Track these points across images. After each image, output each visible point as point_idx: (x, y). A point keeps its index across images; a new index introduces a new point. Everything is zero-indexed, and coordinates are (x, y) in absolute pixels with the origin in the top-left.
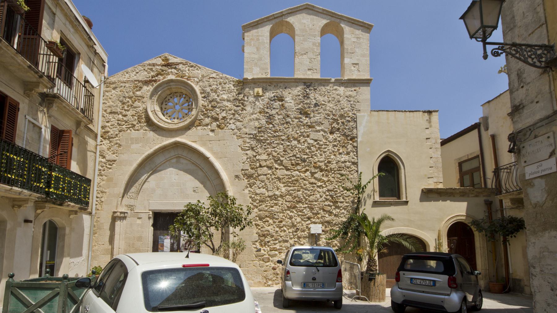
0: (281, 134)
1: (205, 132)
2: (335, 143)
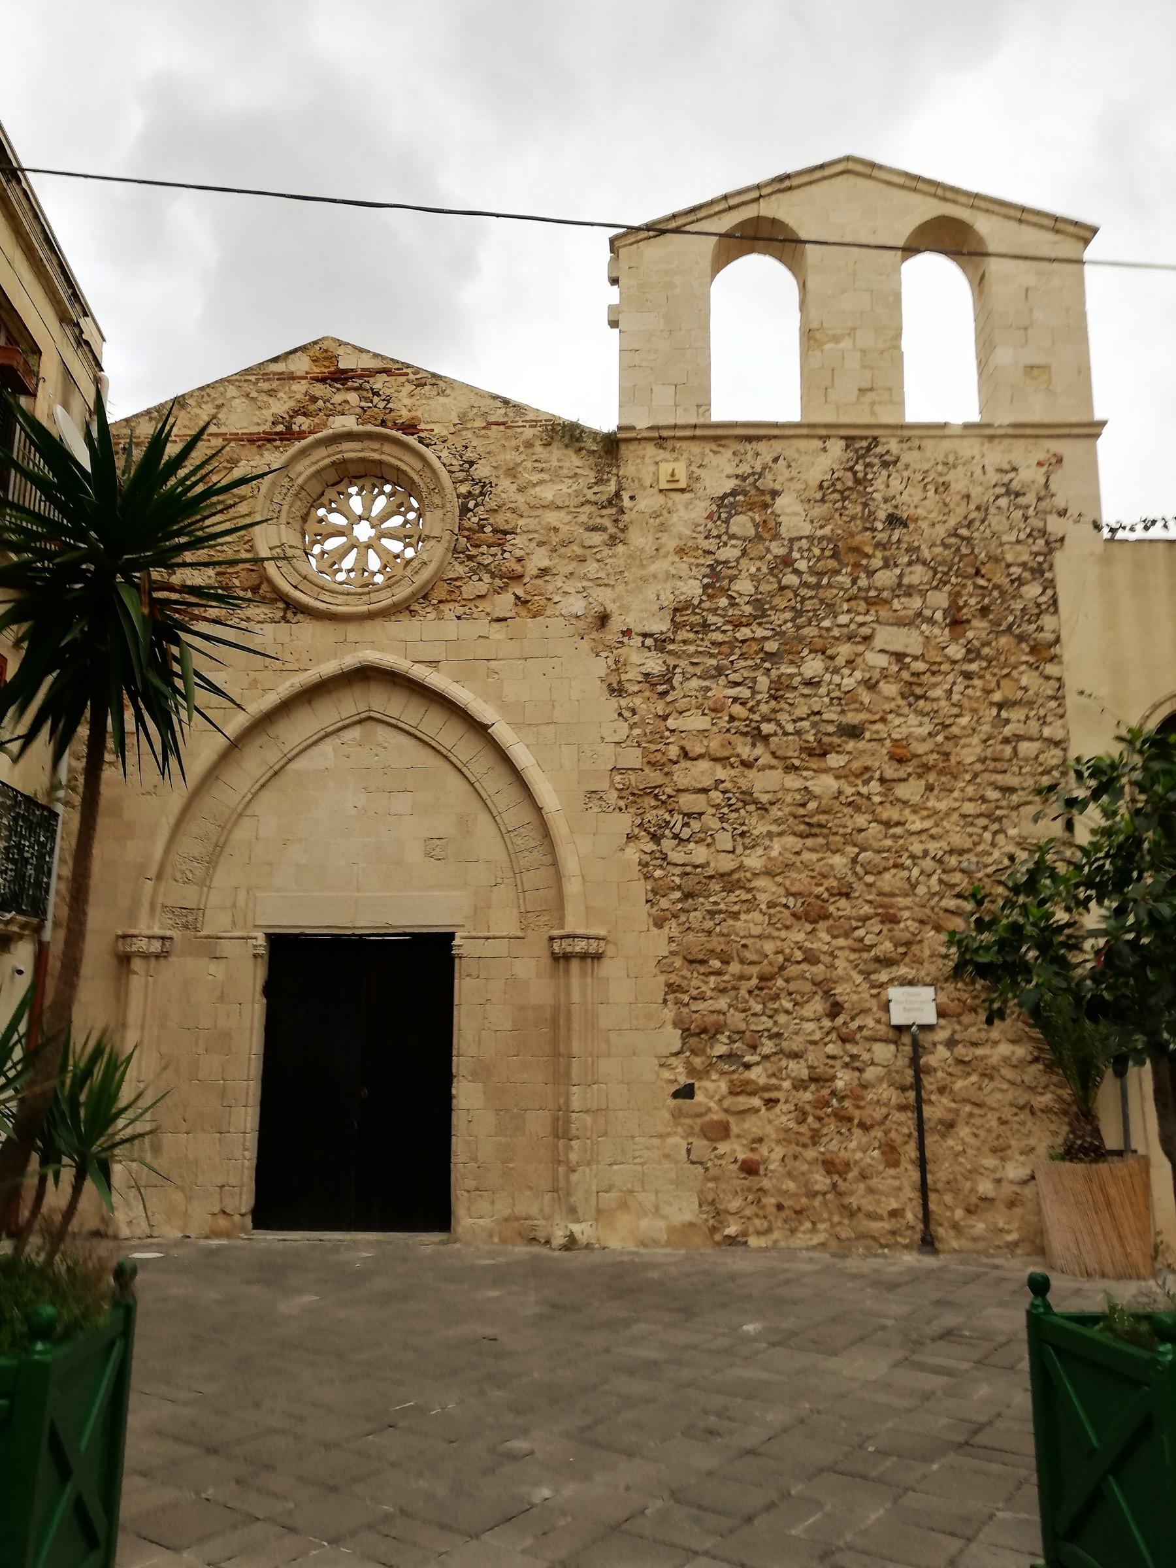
0: (760, 633)
1: (469, 629)
2: (974, 667)
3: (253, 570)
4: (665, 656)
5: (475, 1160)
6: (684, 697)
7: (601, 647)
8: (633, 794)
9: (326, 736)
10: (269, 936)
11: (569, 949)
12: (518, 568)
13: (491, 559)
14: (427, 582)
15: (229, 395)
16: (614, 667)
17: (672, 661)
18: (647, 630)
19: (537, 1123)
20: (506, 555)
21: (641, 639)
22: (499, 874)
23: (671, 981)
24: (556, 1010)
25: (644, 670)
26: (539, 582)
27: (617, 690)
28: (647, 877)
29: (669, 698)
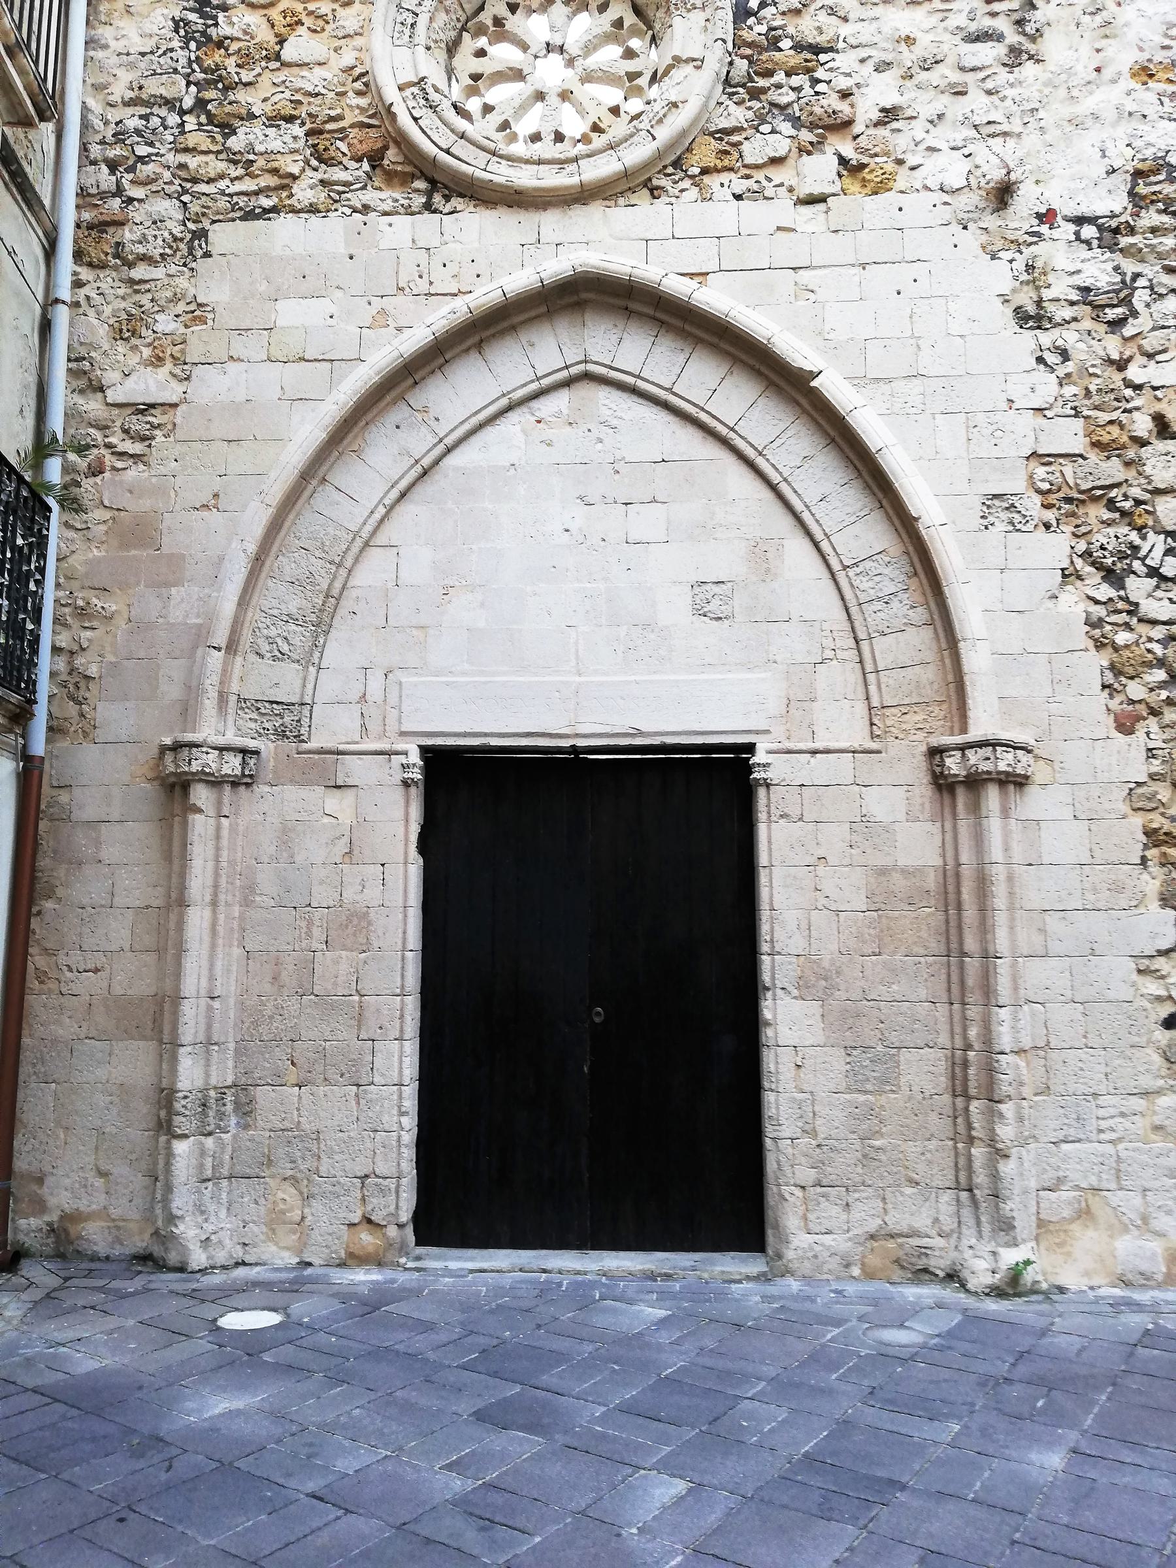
3: (370, 126)
4: (1118, 257)
5: (814, 1133)
6: (1154, 329)
7: (999, 244)
8: (1068, 500)
9: (509, 408)
10: (425, 750)
11: (985, 766)
12: (843, 107)
13: (792, 96)
14: (683, 133)
16: (1025, 277)
17: (1130, 267)
18: (1085, 210)
19: (923, 1071)
20: (820, 87)
21: (1072, 227)
22: (828, 643)
23: (1155, 825)
24: (950, 877)
25: (1078, 280)
26: (882, 132)
27: (1032, 318)
28: (1099, 645)
29: (1128, 331)
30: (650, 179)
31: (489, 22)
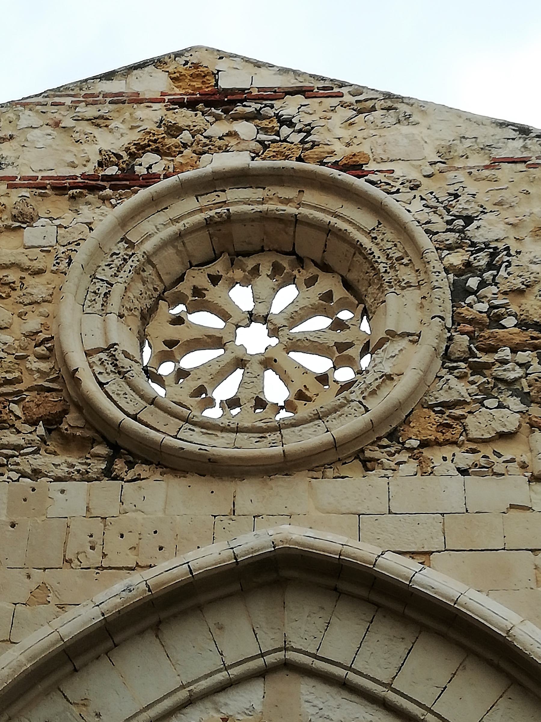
1: (485, 492)
3: (49, 390)
9: (191, 701)
13: (519, 372)
14: (399, 406)
15: (23, 123)
30: (362, 451)
31: (189, 292)
